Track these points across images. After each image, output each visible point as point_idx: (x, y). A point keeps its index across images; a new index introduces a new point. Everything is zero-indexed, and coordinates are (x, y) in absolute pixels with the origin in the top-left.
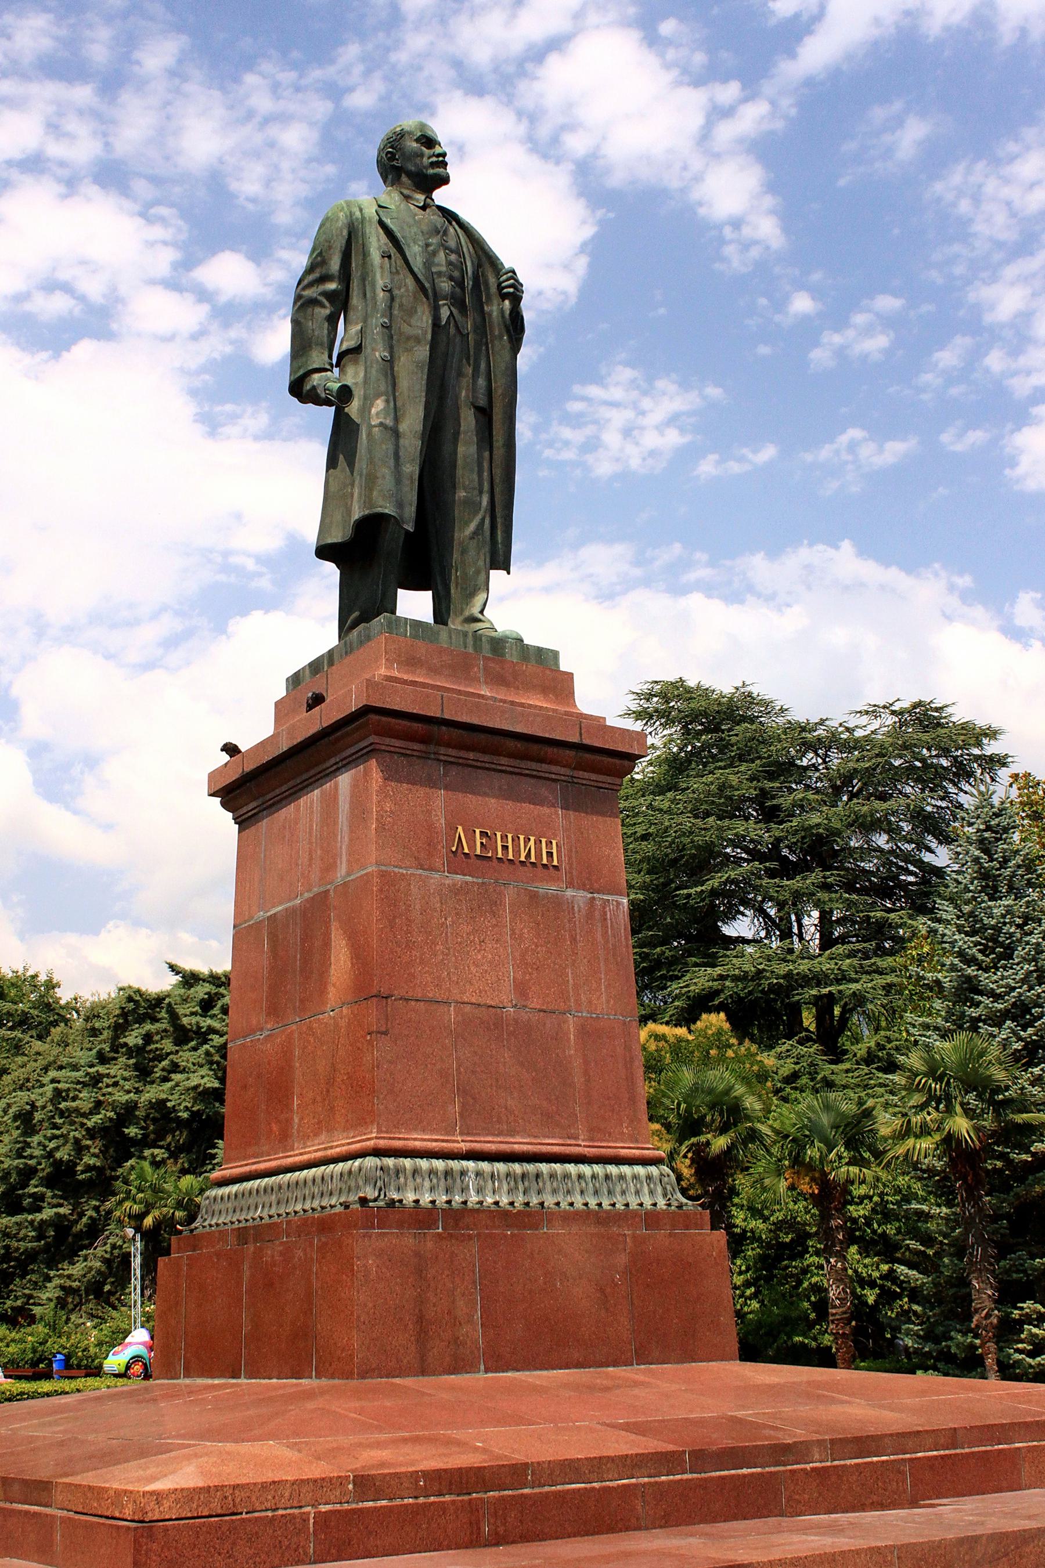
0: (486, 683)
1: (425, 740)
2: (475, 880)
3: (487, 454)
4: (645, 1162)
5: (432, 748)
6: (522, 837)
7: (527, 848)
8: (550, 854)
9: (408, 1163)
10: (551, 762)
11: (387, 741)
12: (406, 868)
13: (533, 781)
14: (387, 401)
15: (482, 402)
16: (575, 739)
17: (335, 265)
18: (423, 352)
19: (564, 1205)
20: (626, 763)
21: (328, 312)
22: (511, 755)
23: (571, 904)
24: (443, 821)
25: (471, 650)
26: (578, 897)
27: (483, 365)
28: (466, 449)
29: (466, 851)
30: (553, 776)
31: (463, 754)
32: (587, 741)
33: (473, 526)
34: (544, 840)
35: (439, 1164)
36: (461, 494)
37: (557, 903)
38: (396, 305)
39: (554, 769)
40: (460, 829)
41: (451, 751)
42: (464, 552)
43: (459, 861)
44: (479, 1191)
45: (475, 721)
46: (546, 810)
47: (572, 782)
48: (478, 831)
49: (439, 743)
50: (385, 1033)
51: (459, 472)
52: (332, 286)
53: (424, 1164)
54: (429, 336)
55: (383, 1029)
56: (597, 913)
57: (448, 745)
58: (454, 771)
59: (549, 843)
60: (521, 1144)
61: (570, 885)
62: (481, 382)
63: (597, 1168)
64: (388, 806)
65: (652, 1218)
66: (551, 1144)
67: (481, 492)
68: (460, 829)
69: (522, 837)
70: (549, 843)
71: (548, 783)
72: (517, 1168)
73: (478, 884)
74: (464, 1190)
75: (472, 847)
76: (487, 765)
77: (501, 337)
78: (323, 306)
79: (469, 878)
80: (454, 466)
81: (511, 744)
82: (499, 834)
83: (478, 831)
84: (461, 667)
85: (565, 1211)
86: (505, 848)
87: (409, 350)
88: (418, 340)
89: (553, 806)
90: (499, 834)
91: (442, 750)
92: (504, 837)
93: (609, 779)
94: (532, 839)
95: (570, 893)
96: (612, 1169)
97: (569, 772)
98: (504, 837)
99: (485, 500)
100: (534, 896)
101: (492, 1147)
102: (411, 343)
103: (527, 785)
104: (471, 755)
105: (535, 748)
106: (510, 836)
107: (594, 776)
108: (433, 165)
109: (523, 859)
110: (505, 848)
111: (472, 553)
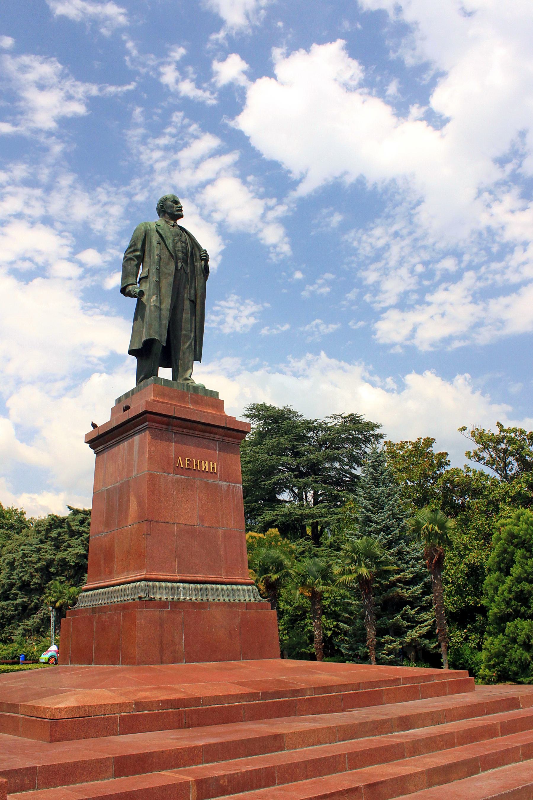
0: (191, 403)
1: (168, 424)
3: (194, 318)
4: (247, 584)
5: (170, 427)
6: (203, 462)
7: (205, 466)
8: (213, 468)
9: (157, 584)
10: (216, 434)
11: (154, 424)
12: (159, 472)
14: (157, 297)
15: (193, 298)
16: (223, 425)
17: (139, 246)
18: (171, 279)
19: (216, 600)
20: (243, 434)
21: (136, 263)
22: (199, 431)
23: (221, 487)
25: (185, 390)
26: (225, 484)
27: (193, 285)
28: (186, 315)
29: (182, 466)
32: (228, 426)
33: (188, 344)
34: (211, 463)
35: (169, 584)
36: (184, 332)
37: (216, 486)
38: (162, 262)
39: (216, 436)
40: (180, 458)
41: (177, 429)
42: (184, 354)
43: (179, 470)
44: (184, 594)
45: (187, 418)
46: (212, 452)
50: (150, 534)
51: (183, 324)
52: (138, 253)
53: (163, 584)
54: (174, 273)
55: (149, 533)
56: (231, 491)
57: (176, 426)
58: (178, 436)
62: (193, 291)
63: (229, 586)
65: (249, 605)
67: (191, 332)
68: (180, 458)
69: (203, 462)
72: (198, 586)
74: (179, 594)
75: (184, 465)
77: (200, 274)
78: (134, 261)
79: (183, 477)
80: (181, 321)
81: (200, 426)
82: (194, 460)
84: (182, 397)
85: (216, 602)
87: (165, 278)
88: (169, 275)
89: (215, 450)
90: (194, 460)
91: (174, 428)
92: (196, 462)
93: (236, 441)
95: (220, 483)
96: (234, 587)
97: (221, 437)
98: (196, 462)
99: (193, 335)
100: (207, 484)
102: (167, 275)
103: (206, 442)
104: (185, 430)
105: (209, 428)
107: (230, 439)
108: (177, 211)
109: (203, 469)
111: (187, 354)
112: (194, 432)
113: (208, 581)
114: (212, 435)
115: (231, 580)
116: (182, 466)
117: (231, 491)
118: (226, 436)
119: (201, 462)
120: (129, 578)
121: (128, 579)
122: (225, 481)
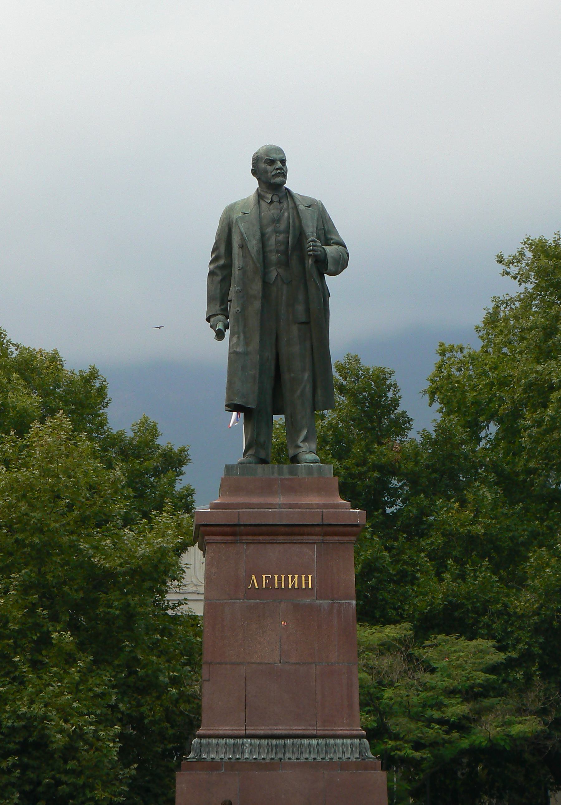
1: (233, 534)
2: (262, 601)
4: (351, 737)
5: (238, 538)
6: (290, 576)
8: (307, 584)
13: (299, 545)
14: (238, 337)
19: (319, 759)
24: (244, 574)
26: (325, 603)
30: (311, 542)
31: (255, 538)
34: (303, 576)
35: (230, 741)
40: (254, 576)
41: (250, 538)
44: (251, 753)
47: (323, 542)
48: (264, 576)
49: (242, 535)
53: (222, 741)
54: (261, 295)
56: (335, 611)
58: (252, 547)
59: (306, 578)
60: (280, 730)
61: (321, 598)
63: (321, 741)
64: (213, 570)
65: (344, 766)
66: (298, 729)
68: (254, 576)
69: (290, 576)
70: (306, 578)
71: (309, 545)
72: (274, 742)
73: (263, 603)
74: (243, 752)
76: (271, 541)
78: (217, 275)
81: (283, 529)
82: (276, 576)
83: (264, 576)
85: (294, 762)
86: (280, 584)
90: (276, 576)
91: (244, 538)
92: (280, 578)
94: (296, 576)
95: (318, 602)
96: (331, 741)
98: (280, 578)
101: (262, 732)
104: (261, 538)
105: (296, 529)
106: (283, 577)
107: (336, 538)
109: (290, 587)
110: (280, 584)
112: (275, 538)
113: (298, 734)
114: (306, 537)
115: (352, 732)
116: (257, 587)
117: (335, 611)
118: (325, 534)
119: (286, 579)
120: (353, 730)
121: (327, 732)
122: (327, 598)
